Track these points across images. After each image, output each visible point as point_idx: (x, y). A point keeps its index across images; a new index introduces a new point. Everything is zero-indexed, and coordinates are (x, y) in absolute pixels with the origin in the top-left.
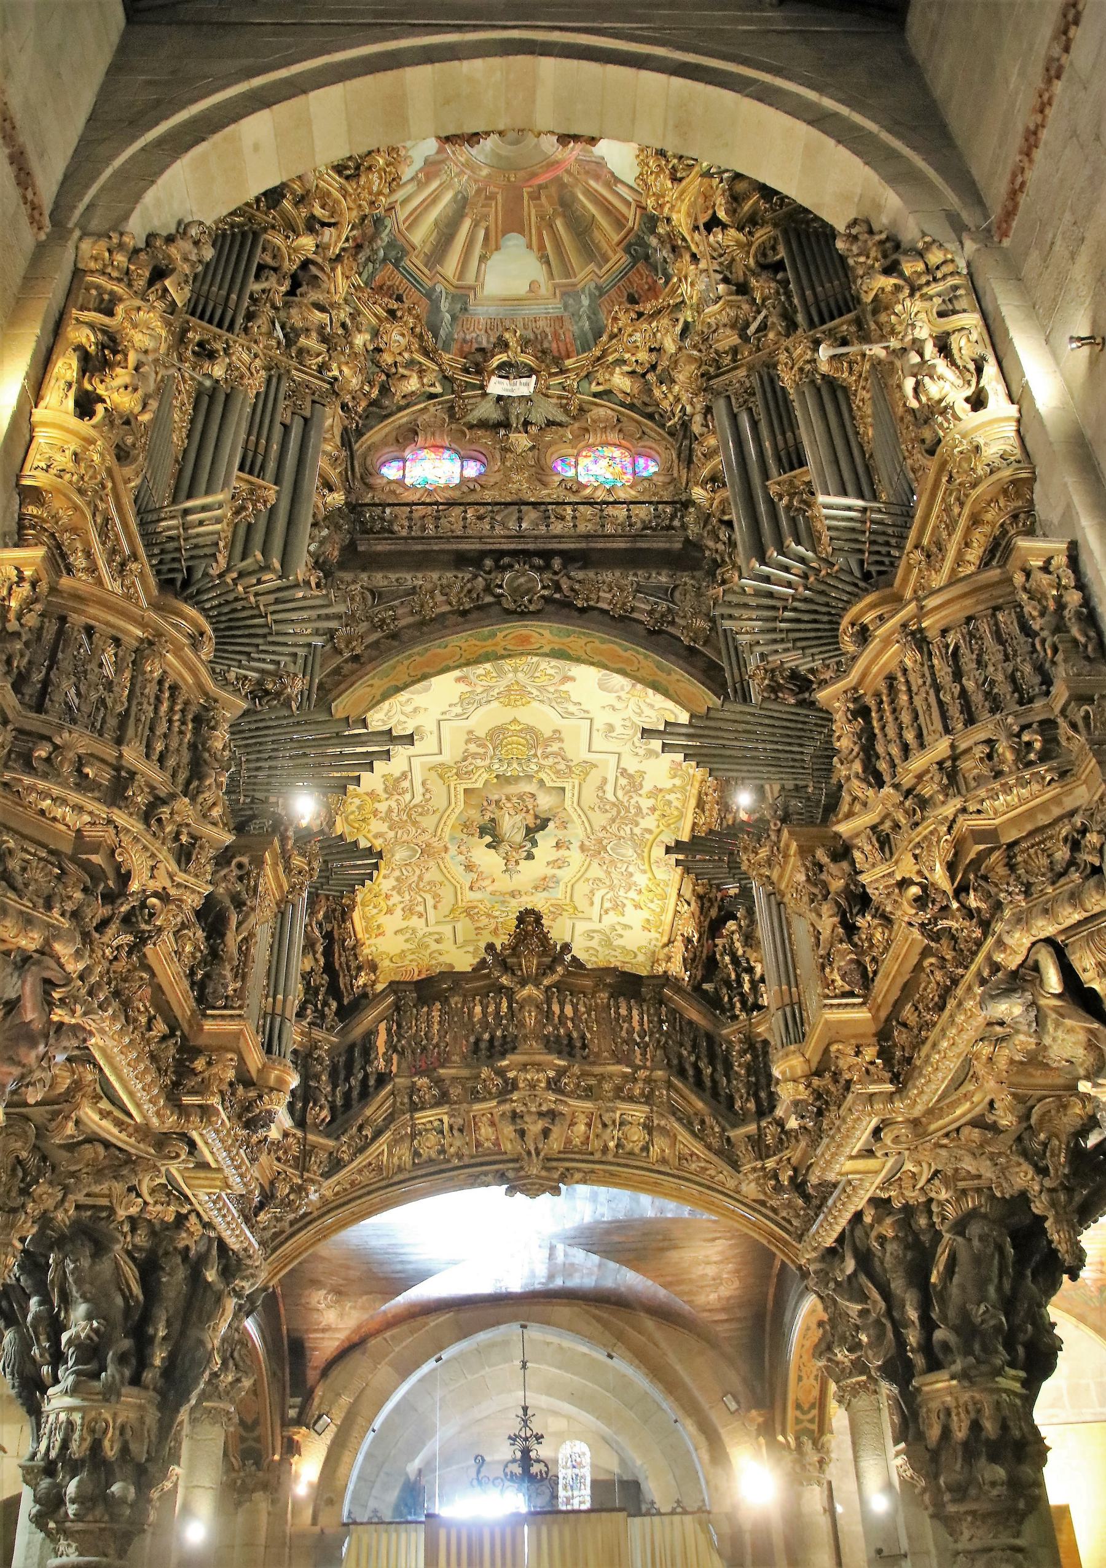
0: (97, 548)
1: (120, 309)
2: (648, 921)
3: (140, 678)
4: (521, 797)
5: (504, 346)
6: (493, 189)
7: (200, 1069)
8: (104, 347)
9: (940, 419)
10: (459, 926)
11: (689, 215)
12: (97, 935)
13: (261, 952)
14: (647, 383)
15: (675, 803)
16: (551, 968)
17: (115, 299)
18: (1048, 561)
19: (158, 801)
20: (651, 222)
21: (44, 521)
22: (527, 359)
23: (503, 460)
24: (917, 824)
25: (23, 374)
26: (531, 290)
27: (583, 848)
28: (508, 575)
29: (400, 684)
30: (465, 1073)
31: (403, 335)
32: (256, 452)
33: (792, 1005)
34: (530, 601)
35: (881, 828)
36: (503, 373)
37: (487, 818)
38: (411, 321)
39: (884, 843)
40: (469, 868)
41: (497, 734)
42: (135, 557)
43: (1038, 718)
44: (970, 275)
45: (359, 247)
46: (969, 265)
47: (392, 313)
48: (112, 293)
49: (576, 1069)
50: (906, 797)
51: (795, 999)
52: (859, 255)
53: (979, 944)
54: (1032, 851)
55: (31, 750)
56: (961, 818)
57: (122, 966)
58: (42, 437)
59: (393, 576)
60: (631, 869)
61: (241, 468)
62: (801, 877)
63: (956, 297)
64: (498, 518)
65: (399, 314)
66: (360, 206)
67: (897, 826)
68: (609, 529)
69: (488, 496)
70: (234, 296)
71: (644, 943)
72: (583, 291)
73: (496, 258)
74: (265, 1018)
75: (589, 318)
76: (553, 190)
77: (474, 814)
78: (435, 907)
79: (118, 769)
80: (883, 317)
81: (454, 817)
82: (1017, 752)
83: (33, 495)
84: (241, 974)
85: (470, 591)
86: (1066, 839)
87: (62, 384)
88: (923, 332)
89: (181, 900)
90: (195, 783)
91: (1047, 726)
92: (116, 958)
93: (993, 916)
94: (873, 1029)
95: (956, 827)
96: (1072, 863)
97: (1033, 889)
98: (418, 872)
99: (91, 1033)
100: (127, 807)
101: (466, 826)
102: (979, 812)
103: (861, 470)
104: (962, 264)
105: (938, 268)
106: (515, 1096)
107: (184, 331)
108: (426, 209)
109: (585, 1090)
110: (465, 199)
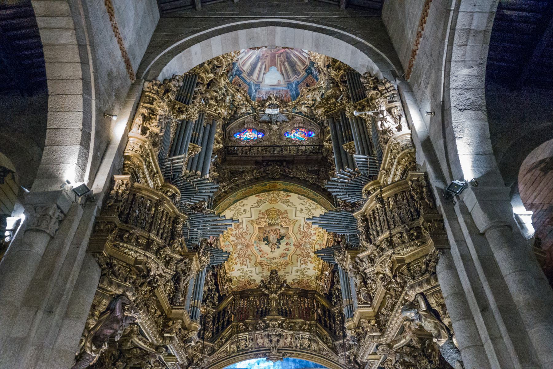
0: (146, 172)
1: (155, 103)
2: (315, 267)
3: (157, 212)
4: (275, 230)
5: (270, 98)
6: (267, 54)
7: (170, 325)
8: (150, 114)
9: (388, 134)
10: (257, 268)
11: (323, 62)
12: (140, 288)
13: (191, 288)
14: (312, 110)
15: (322, 232)
16: (280, 288)
17: (154, 99)
18: (418, 178)
19: (160, 248)
20: (313, 63)
21: (131, 165)
22: (277, 103)
23: (270, 132)
24: (380, 256)
25: (126, 123)
26: (278, 83)
27: (294, 245)
28: (270, 168)
29: (238, 199)
30: (253, 321)
31: (241, 96)
32: (195, 136)
33: (350, 305)
34: (277, 175)
35: (371, 256)
36: (270, 107)
37: (265, 236)
38: (243, 92)
39: (372, 260)
40: (260, 251)
41: (268, 211)
42: (158, 172)
43: (415, 226)
44: (398, 90)
45: (228, 72)
46: (398, 87)
47: (238, 90)
48: (153, 98)
49: (287, 320)
50: (377, 248)
51: (351, 303)
52: (366, 83)
53: (401, 293)
54: (415, 266)
55: (123, 235)
56: (393, 256)
57: (147, 296)
58: (131, 140)
59: (237, 167)
60: (309, 251)
61: (191, 142)
62: (351, 267)
63: (394, 97)
64: (268, 150)
65: (240, 90)
66: (228, 61)
67: (375, 256)
68: (300, 153)
69: (265, 143)
70: (189, 94)
71: (314, 274)
72: (293, 83)
73: (268, 73)
74: (191, 308)
75: (295, 91)
76: (285, 54)
77: (261, 235)
78: (250, 262)
79: (148, 239)
80: (373, 101)
81: (255, 236)
82: (409, 236)
83: (128, 158)
84: (184, 295)
85: (259, 172)
86: (425, 263)
87: (137, 125)
88: (383, 108)
89: (166, 277)
90: (172, 241)
91: (418, 229)
92: (146, 294)
93: (404, 284)
94: (373, 315)
95: (392, 258)
96: (427, 270)
97: (416, 278)
98: (245, 252)
99: (136, 319)
100: (151, 251)
101: (259, 238)
102: (398, 254)
103: (369, 144)
104: (396, 87)
105: (389, 88)
106: (269, 329)
107: (174, 105)
109: (290, 327)
110: (259, 57)
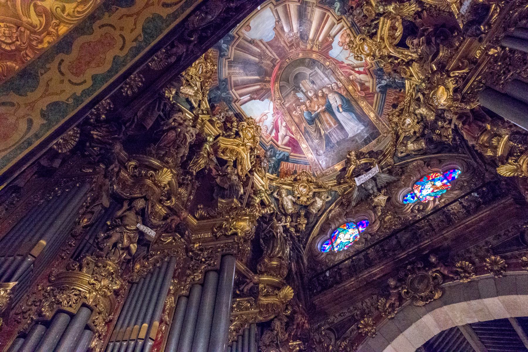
26: (248, 25)
76: (268, 69)
108: (319, 25)
